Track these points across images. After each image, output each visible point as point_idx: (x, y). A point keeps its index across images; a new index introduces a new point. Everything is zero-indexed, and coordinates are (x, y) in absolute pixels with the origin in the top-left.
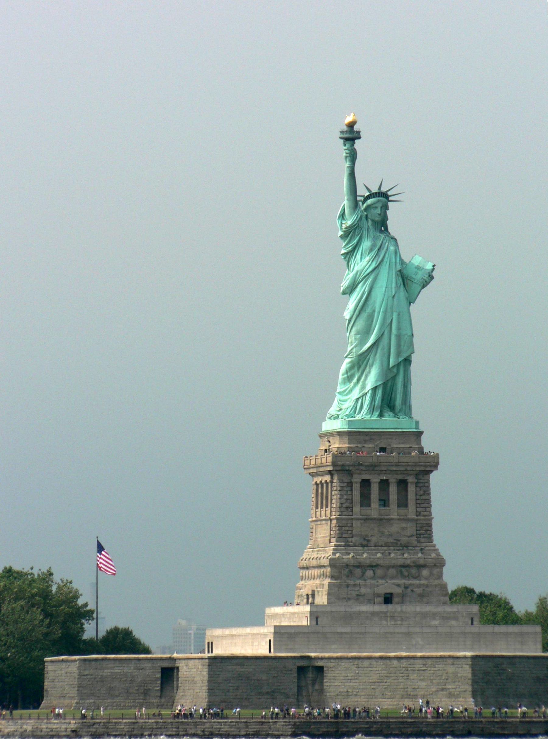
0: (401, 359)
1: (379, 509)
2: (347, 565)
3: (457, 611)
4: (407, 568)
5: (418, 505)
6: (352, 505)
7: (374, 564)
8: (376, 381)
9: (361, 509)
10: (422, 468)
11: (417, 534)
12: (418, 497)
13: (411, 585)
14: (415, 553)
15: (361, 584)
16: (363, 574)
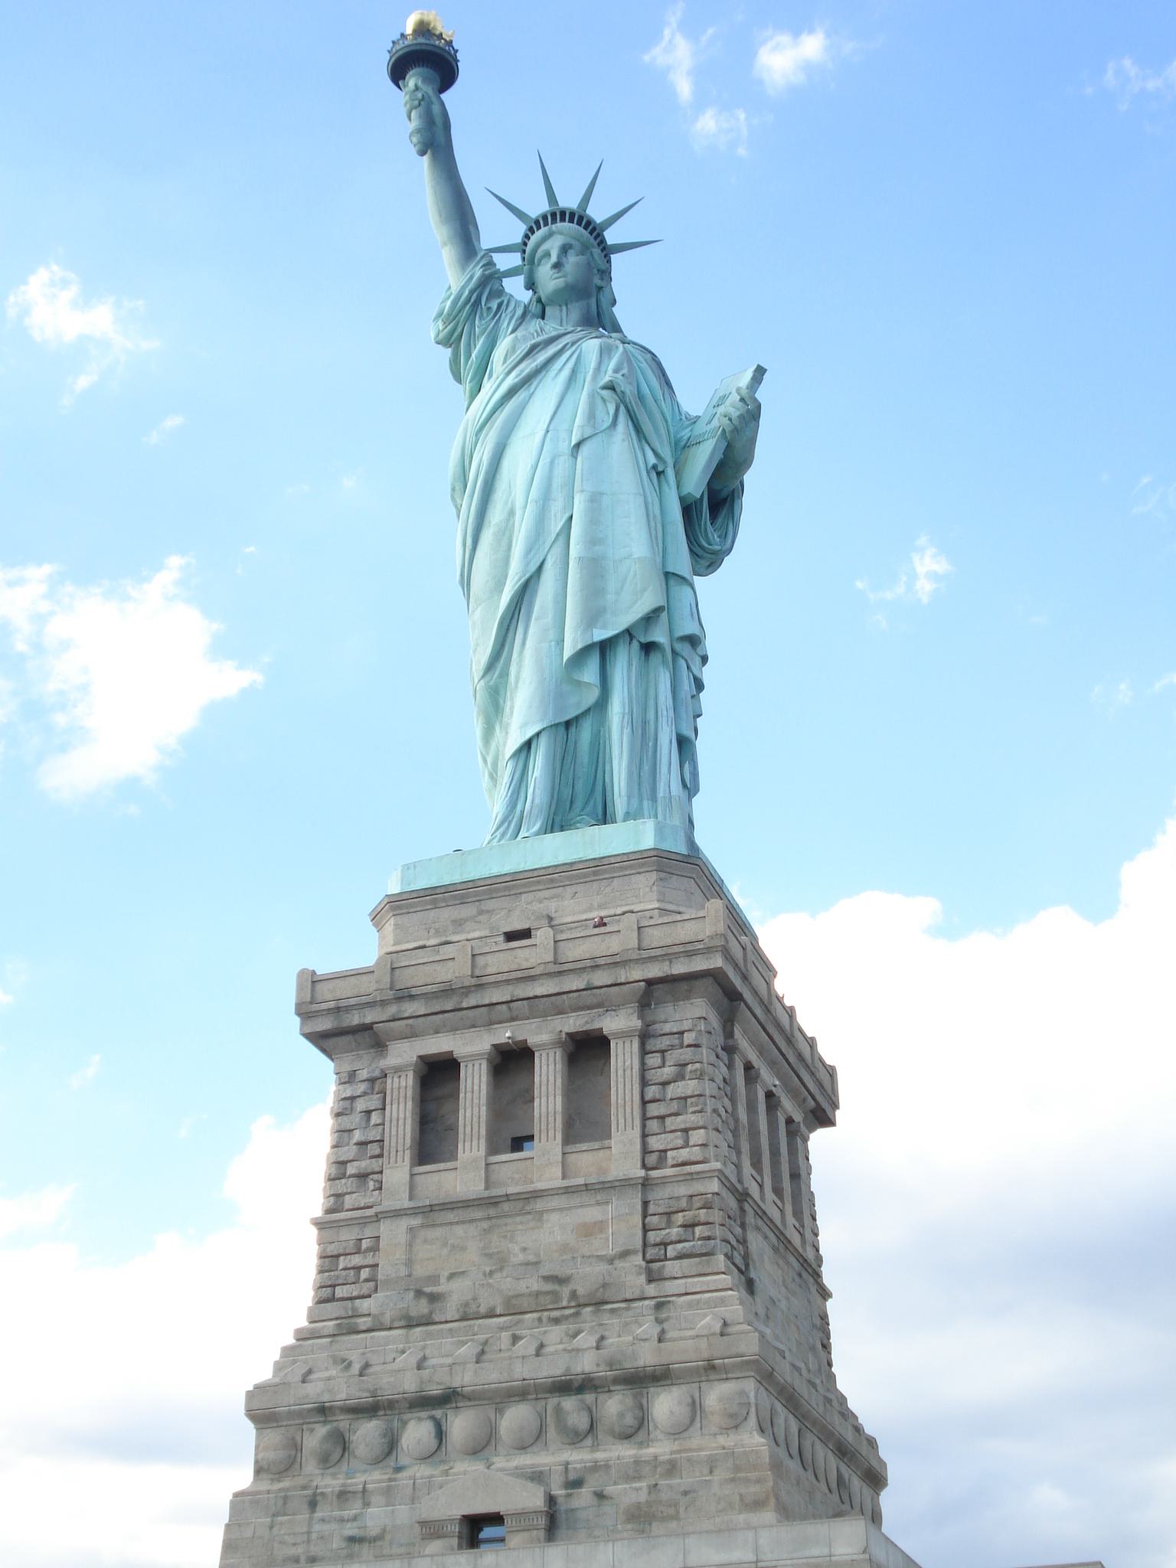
0: (600, 635)
1: (487, 1165)
2: (323, 1411)
3: (751, 1557)
4: (589, 1398)
5: (654, 1125)
6: (380, 1160)
7: (435, 1390)
8: (524, 726)
9: (412, 1175)
10: (655, 971)
11: (645, 1245)
12: (652, 1092)
13: (596, 1467)
14: (627, 1324)
15: (369, 1486)
16: (392, 1445)
